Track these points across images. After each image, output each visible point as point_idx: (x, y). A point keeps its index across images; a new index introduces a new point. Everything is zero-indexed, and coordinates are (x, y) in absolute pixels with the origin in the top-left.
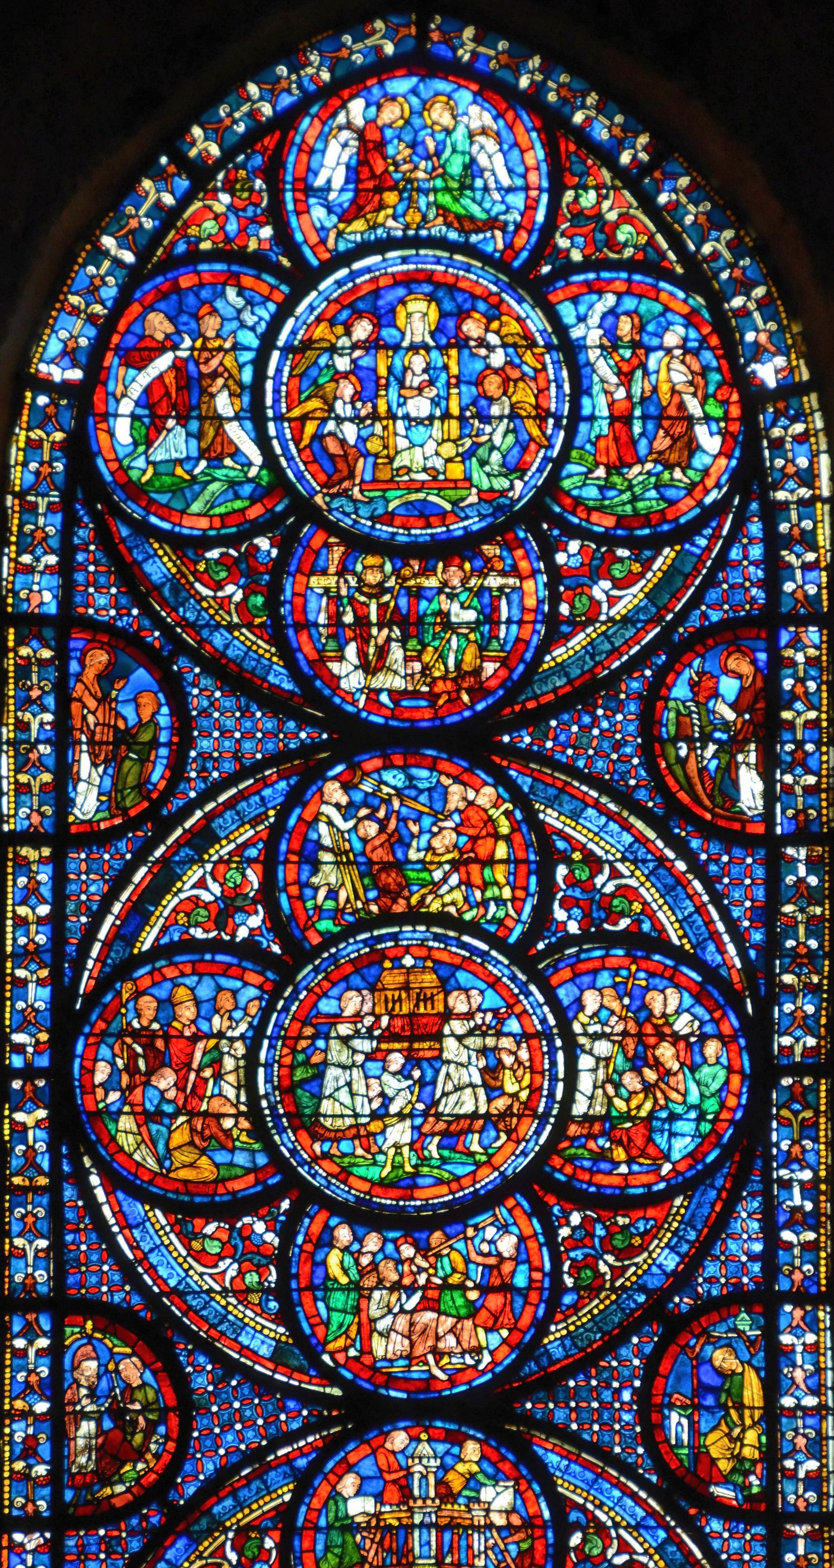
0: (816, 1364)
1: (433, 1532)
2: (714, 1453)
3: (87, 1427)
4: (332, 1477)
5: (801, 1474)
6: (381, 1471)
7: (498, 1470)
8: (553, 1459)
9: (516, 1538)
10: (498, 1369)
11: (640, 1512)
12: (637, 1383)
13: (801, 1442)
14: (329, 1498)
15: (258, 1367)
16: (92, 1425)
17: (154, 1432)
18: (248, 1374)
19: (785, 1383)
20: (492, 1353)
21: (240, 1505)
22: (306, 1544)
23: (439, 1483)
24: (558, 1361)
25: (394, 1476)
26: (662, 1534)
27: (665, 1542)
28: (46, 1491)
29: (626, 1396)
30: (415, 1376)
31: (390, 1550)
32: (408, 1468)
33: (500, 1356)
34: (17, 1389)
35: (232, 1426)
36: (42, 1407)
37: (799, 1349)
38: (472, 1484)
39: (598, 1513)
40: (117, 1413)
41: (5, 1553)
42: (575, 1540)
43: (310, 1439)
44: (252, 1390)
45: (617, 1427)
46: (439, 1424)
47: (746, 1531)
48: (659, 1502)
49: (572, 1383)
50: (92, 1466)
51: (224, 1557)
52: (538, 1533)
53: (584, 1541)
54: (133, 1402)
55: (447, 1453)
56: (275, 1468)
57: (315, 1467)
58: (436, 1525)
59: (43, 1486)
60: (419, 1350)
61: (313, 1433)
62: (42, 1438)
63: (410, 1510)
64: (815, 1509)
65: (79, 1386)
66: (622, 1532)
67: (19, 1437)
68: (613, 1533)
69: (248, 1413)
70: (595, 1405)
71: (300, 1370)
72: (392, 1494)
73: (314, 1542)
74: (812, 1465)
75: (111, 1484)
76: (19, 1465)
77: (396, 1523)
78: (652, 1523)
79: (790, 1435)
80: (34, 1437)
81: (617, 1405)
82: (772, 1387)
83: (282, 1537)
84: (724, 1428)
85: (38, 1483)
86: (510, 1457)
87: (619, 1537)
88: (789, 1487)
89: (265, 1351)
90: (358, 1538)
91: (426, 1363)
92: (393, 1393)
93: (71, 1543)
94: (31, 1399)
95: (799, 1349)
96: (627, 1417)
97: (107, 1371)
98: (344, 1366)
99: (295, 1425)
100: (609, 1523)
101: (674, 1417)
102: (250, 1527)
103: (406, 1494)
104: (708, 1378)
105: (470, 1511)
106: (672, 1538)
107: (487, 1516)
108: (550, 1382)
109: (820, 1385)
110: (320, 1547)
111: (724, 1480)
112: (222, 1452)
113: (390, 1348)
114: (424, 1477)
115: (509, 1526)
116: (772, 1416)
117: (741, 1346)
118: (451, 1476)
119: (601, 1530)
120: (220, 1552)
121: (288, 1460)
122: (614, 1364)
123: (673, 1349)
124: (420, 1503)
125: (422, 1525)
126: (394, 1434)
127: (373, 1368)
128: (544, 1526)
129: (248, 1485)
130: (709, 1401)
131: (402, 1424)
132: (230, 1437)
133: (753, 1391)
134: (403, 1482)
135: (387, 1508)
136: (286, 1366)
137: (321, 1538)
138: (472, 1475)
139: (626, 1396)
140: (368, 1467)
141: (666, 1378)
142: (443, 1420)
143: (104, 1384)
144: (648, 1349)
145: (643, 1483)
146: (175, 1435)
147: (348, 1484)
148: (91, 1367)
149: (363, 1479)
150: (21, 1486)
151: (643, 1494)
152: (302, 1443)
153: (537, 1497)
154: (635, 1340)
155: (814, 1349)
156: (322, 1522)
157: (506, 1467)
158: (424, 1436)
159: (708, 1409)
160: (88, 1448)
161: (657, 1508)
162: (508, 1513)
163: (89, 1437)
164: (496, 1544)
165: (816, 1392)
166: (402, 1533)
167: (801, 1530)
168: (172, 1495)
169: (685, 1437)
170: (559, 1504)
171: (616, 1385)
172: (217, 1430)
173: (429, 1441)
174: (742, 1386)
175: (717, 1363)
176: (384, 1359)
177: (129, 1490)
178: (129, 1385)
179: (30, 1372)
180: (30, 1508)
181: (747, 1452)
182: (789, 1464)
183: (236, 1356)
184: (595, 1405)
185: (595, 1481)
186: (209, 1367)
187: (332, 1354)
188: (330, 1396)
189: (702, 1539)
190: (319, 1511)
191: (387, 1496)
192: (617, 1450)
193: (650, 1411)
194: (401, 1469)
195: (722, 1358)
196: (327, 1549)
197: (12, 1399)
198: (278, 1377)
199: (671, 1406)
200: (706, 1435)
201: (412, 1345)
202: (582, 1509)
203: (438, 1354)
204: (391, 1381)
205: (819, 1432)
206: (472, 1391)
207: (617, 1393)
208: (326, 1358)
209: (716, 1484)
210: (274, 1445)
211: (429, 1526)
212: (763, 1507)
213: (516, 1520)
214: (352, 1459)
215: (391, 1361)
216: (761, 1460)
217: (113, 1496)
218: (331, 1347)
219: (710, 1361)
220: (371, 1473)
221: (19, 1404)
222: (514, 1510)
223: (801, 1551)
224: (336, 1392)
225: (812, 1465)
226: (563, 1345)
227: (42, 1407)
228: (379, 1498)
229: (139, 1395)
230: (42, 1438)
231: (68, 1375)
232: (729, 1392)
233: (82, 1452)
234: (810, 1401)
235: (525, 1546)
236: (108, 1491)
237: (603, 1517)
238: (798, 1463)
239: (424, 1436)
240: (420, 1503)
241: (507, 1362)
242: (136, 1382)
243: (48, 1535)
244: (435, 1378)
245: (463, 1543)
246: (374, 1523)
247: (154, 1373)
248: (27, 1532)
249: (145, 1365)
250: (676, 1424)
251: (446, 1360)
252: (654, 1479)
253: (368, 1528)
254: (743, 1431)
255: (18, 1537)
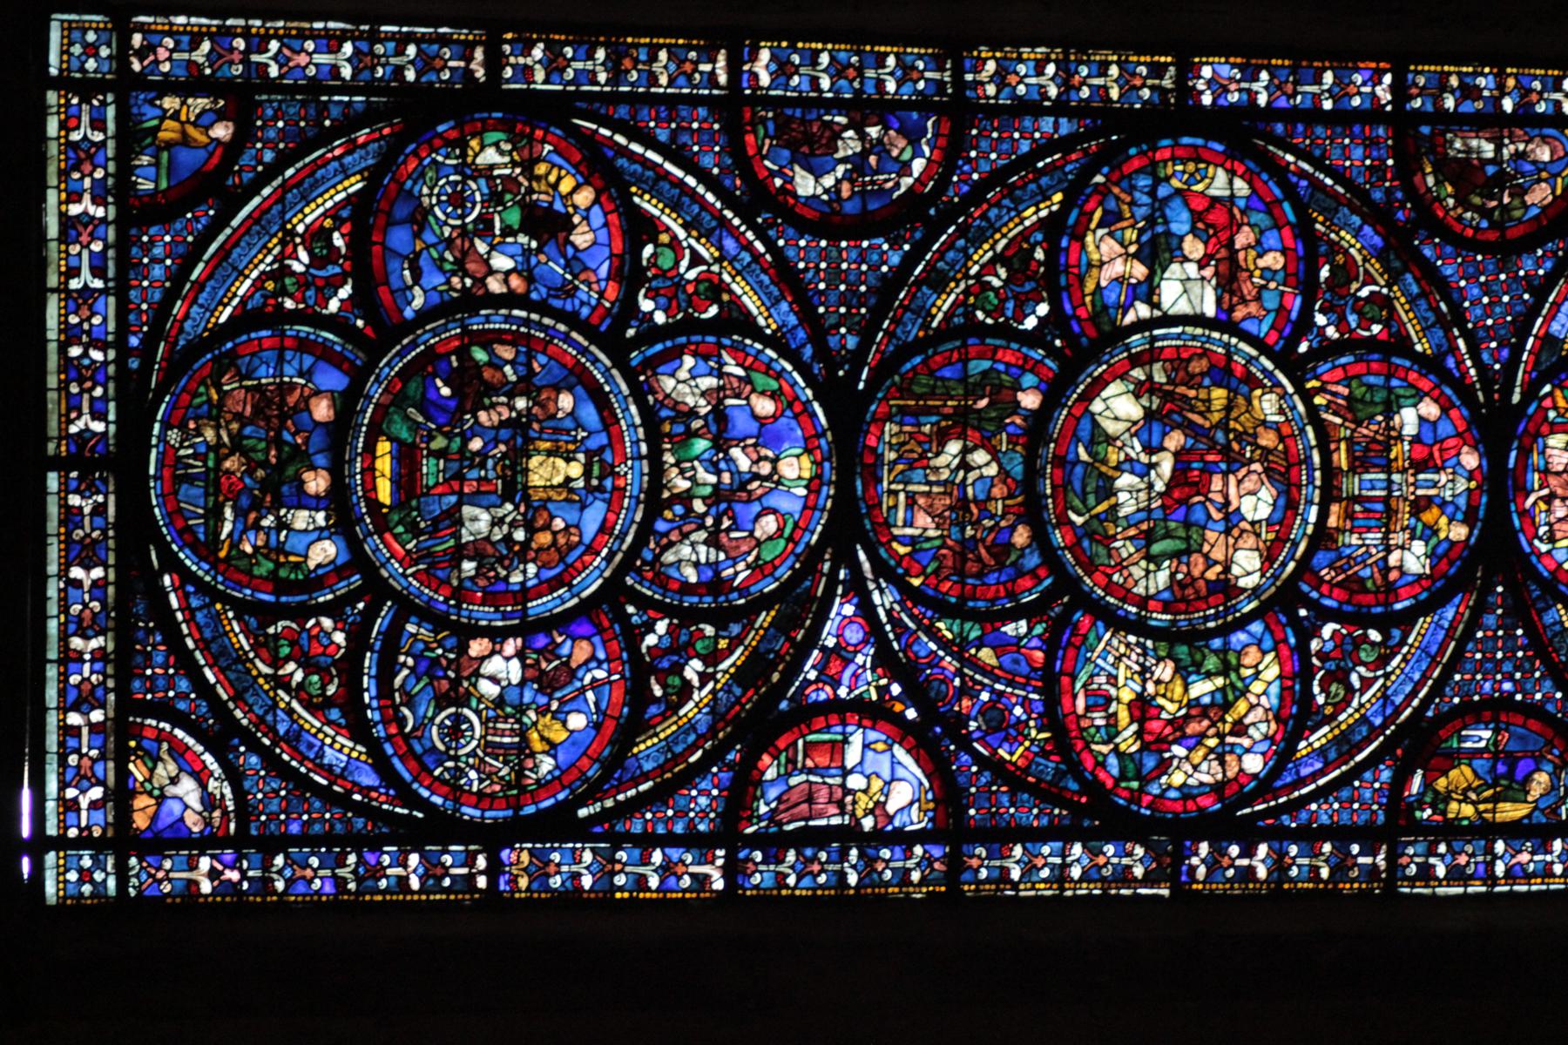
0: (1534, 875)
1: (1383, 493)
2: (1453, 773)
3: (1488, 149)
4: (1436, 392)
5: (1432, 860)
6: (1442, 441)
7: (1440, 558)
8: (1450, 613)
9: (1377, 575)
10: (1534, 559)
11: (1398, 700)
12: (1519, 697)
13: (1463, 860)
14: (1418, 390)
15: (1540, 320)
16: (1490, 155)
17: (1482, 217)
18: (1534, 311)
19: (1516, 844)
20: (1549, 552)
21: (1412, 300)
22: (1374, 366)
23: (1429, 499)
24: (1541, 618)
25: (1437, 454)
26: (1378, 721)
27: (1371, 724)
28: (1429, 108)
29: (1507, 686)
30: (1529, 476)
31: (1367, 449)
32: (1444, 469)
33: (1546, 561)
34: (1525, 81)
35: (1485, 294)
36: (1508, 105)
37: (1549, 858)
38: (1428, 532)
39: (1399, 658)
40: (1501, 179)
41: (1373, 65)
42: (1374, 635)
43: (1472, 372)
44: (1520, 314)
45: (1479, 677)
46: (1484, 500)
47: (1380, 805)
48: (1408, 718)
49: (1520, 632)
50: (1452, 153)
51: (1364, 284)
52: (1381, 597)
53: (1373, 644)
54: (1510, 195)
55: (1457, 508)
56: (1446, 336)
57: (1445, 376)
58: (1389, 496)
59: (1434, 104)
60: (1553, 481)
61: (1479, 374)
62: (1480, 105)
63: (1404, 471)
64: (1399, 874)
65: (1527, 142)
66: (1381, 681)
67: (1481, 81)
68: (1380, 673)
69: (1498, 310)
70: (1499, 655)
71: (1537, 363)
72: (1421, 453)
73: (1377, 374)
74: (1441, 871)
75: (1434, 172)
76: (1454, 81)
77: (1392, 456)
78: (1389, 711)
79: (1469, 849)
80: (1480, 97)
81: (1499, 677)
82: (1515, 832)
83: (1382, 342)
84: (1476, 783)
85: (1438, 99)
86: (1452, 571)
87: (1376, 678)
88: (1421, 848)
89: (1555, 327)
90: (1380, 418)
91: (1541, 488)
92: (1513, 454)
93: (1381, 131)
94: (1516, 94)
95: (1549, 858)
96: (1487, 686)
97: (1540, 171)
98: (1539, 406)
99: (1485, 356)
100: (1389, 669)
101: (1487, 734)
102: (1392, 310)
103: (1420, 466)
104: (1523, 767)
105: (1403, 530)
106: (1374, 732)
107: (1398, 547)
108: (1521, 611)
109: (1514, 878)
110: (1372, 380)
111: (1428, 784)
112: (1463, 283)
113: (1555, 452)
114: (1435, 484)
115: (1388, 569)
116: (1486, 831)
117: (1551, 800)
118: (1435, 511)
119: (1383, 661)
120: (1369, 280)
121: (1454, 349)
122: (1537, 674)
123: (1550, 733)
124: (1411, 480)
125: (1390, 482)
126: (1476, 455)
127: (1538, 435)
128: (1388, 604)
129: (1431, 308)
130: (1501, 769)
131: (1484, 463)
132: (1476, 291)
133: (1510, 811)
134: (1431, 464)
135: (1407, 447)
136: (1541, 349)
137: (1379, 381)
138: (1436, 533)
139: (1507, 686)
140: (1445, 429)
141: (1523, 726)
142: (1488, 504)
143: (1528, 167)
144: (1550, 707)
145: (1426, 703)
146: (1479, 237)
147: (1430, 409)
148: (1544, 154)
149: (1434, 424)
150: (1434, 83)
151: (1415, 703)
152: (1469, 363)
153: (1415, 597)
154: (1559, 695)
155: (1547, 872)
156: (1395, 382)
157: (1444, 565)
158: (1473, 484)
159: (1494, 768)
160: (1469, 150)
161: (1403, 717)
162: (1400, 568)
163: (1479, 152)
164: (1371, 556)
165: (1510, 875)
166: (1383, 462)
167: (1381, 860)
168: (1423, 233)
169: (1468, 745)
170: (1407, 620)
171: (1518, 675)
172: (1482, 279)
173: (1468, 489)
174: (1514, 801)
175: (1536, 776)
176: (1546, 446)
177: (1429, 190)
178: (1526, 193)
179: (1540, 93)
180: (1414, 91)
181: (1454, 806)
182: (1442, 848)
183: (1551, 299)
184: (1499, 655)
185: (1428, 654)
186: (1541, 272)
187: (1551, 394)
188: (1512, 393)
189: (1372, 762)
190: (1405, 380)
191: (1418, 448)
192: (1457, 677)
193: (1493, 710)
194: (1444, 461)
195: (1542, 779)
196: (1370, 387)
197: (1516, 76)
198: (1531, 340)
199: (1496, 731)
200: (1470, 765)
201: (1558, 474)
202: (1403, 642)
203: (1548, 500)
204: (1525, 453)
205: (1472, 877)
206: (1515, 533)
207: (1509, 677)
208: (1547, 388)
209: (1424, 776)
210: (1466, 334)
211: (1389, 488)
212: (1402, 822)
213: (1393, 575)
214: (1454, 413)
215: (1543, 452)
216: (1446, 820)
217: (1424, 175)
218: (1558, 393)
219: (1538, 770)
220: (1440, 431)
221: (1511, 82)
222: (1403, 573)
223: (1361, 860)
224: (1516, 398)
225: (1441, 871)
226: (1554, 624)
227: (1508, 105)
228: (1416, 440)
229: (1516, 202)
230: (1480, 105)
231: (1536, 131)
232: (1508, 788)
233: (1465, 144)
234: (1500, 869)
235: (1369, 584)
236: (1429, 170)
237: (1395, 663)
238: (1442, 856)
239: (1473, 484)
240: (1411, 480)
241: (1540, 567)
242: (1529, 199)
243: (1389, 108)
244: (1527, 496)
245: (1373, 523)
246: (1393, 433)
247: (1536, 217)
248: (1393, 88)
249: (1544, 209)
250: (1481, 736)
251: (1543, 506)
252: (1430, 714)
253: (1389, 428)
254: (1473, 803)
255: (1388, 79)
